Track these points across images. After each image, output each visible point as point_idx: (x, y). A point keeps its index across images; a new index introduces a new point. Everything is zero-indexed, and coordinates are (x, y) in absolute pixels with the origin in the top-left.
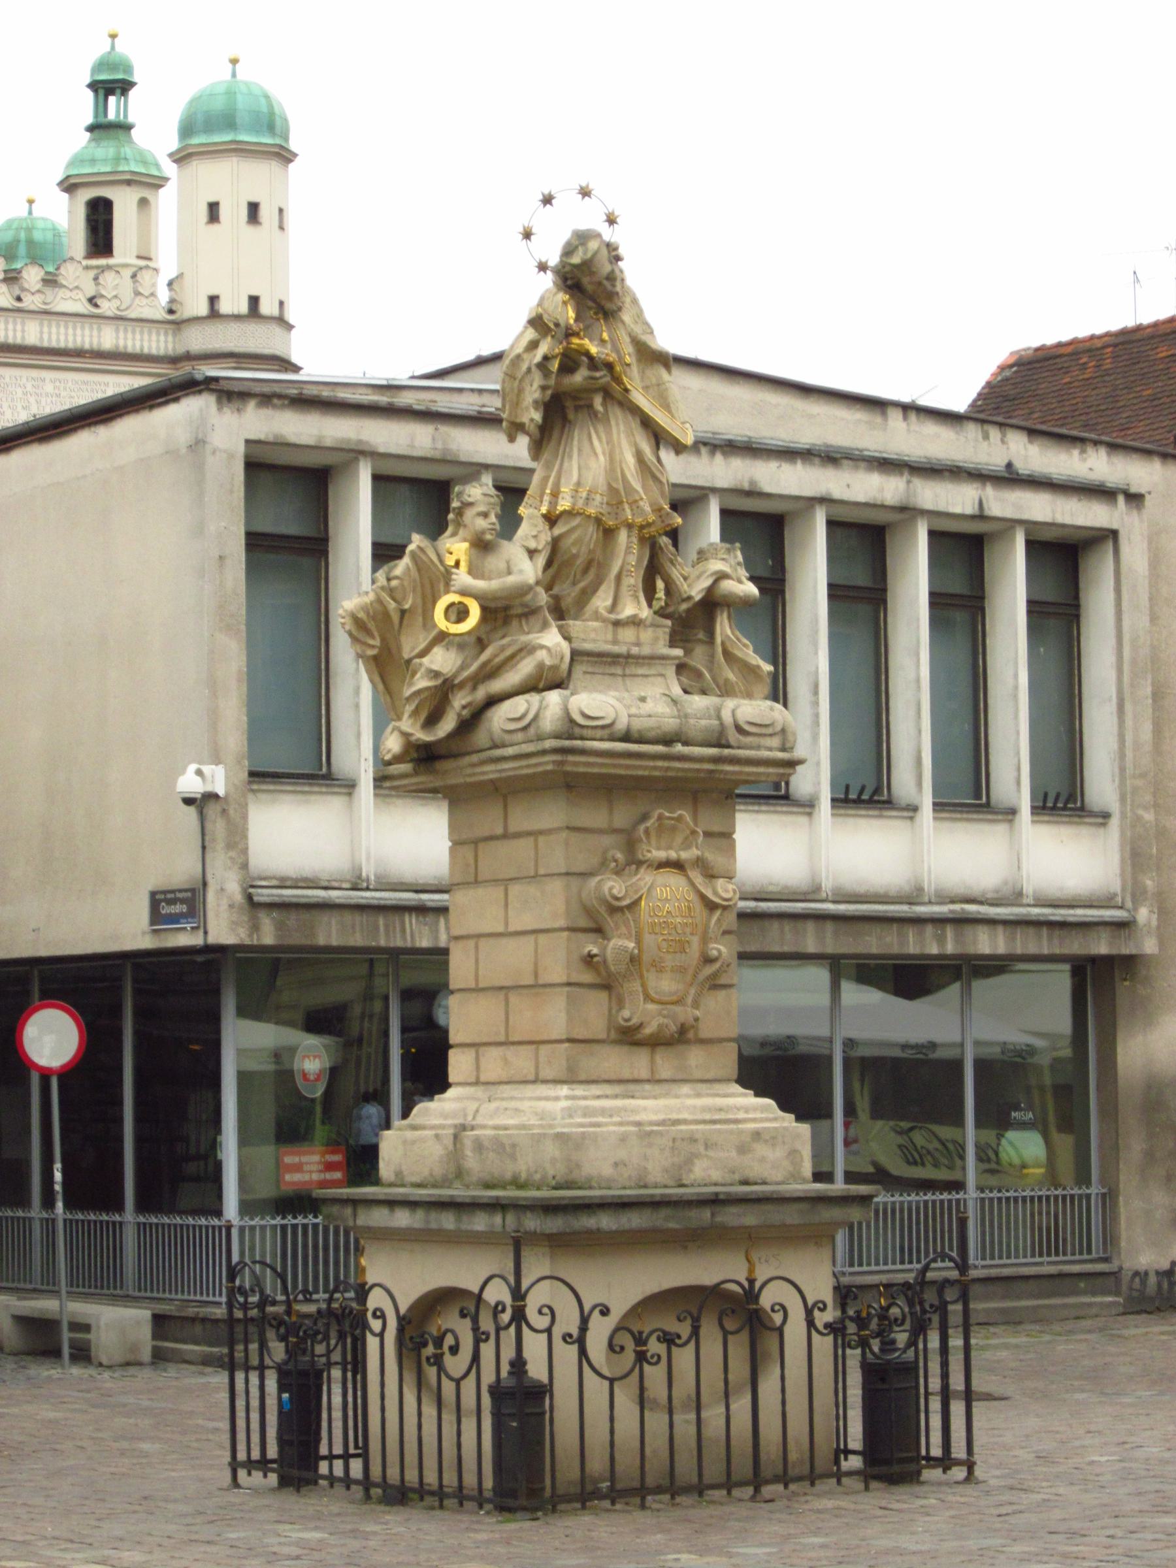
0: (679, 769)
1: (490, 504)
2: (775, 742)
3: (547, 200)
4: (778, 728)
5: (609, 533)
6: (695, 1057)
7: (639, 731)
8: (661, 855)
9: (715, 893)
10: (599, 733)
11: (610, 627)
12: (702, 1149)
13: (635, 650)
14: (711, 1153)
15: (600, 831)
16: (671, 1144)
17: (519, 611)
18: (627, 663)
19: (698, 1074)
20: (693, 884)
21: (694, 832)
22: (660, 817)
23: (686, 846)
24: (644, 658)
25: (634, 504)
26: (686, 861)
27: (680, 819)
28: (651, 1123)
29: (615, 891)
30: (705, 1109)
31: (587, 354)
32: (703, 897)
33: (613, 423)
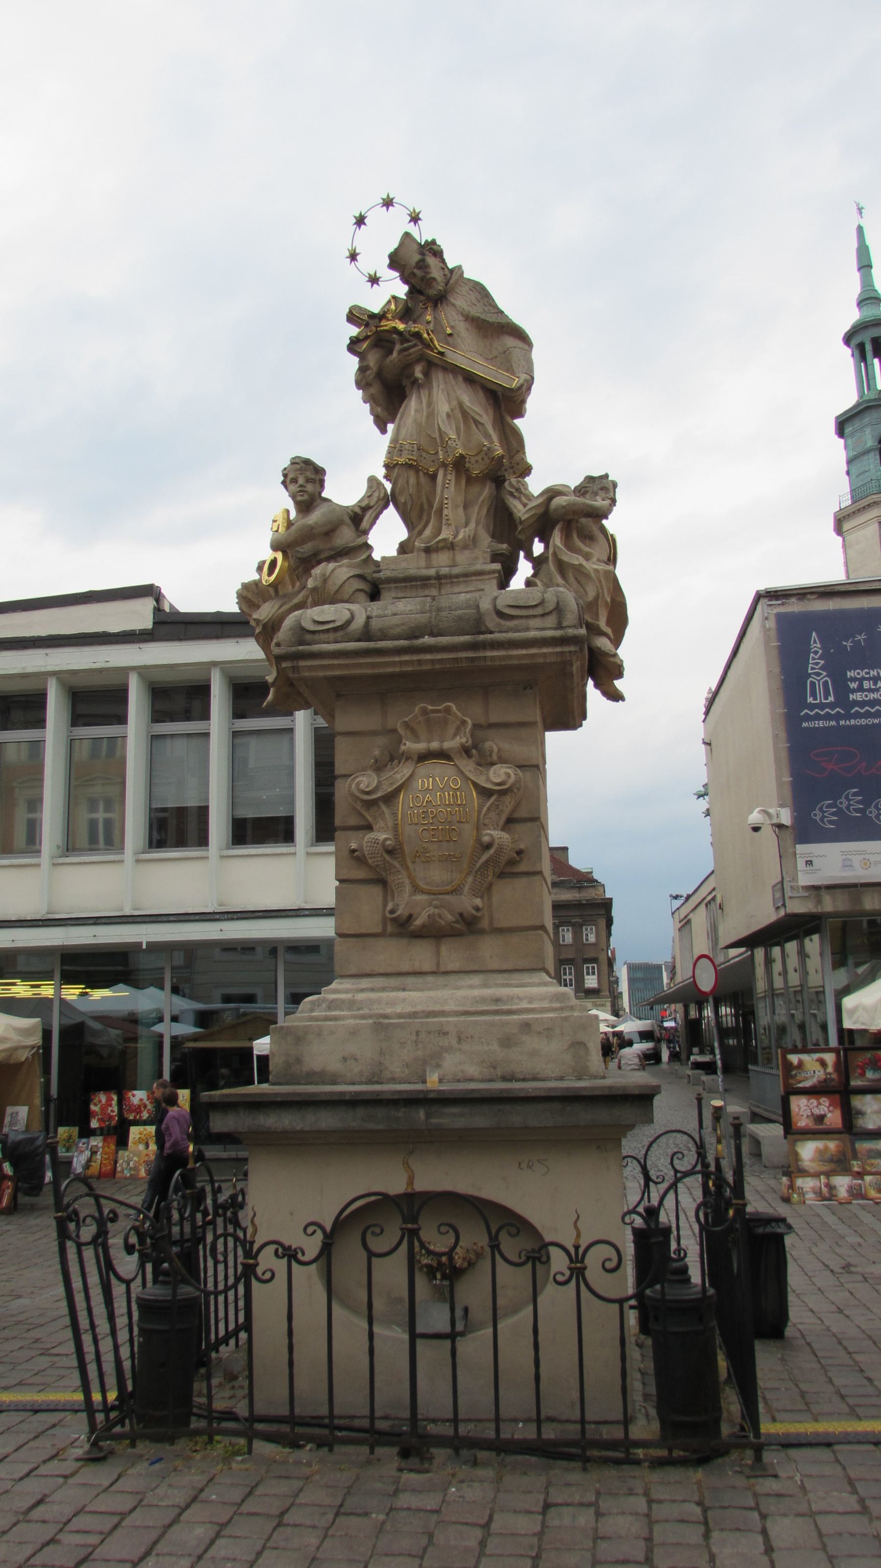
0: (432, 661)
1: (297, 470)
2: (551, 621)
3: (360, 221)
4: (550, 606)
5: (433, 477)
6: (489, 949)
7: (381, 630)
8: (421, 746)
9: (488, 780)
10: (332, 636)
11: (423, 554)
12: (454, 1043)
13: (444, 571)
14: (465, 1047)
15: (374, 733)
16: (414, 1038)
17: (326, 554)
18: (441, 584)
19: (495, 966)
20: (461, 773)
21: (464, 722)
22: (424, 712)
23: (455, 735)
24: (457, 576)
25: (445, 447)
26: (451, 749)
27: (448, 710)
28: (400, 1016)
29: (362, 786)
30: (483, 1000)
31: (395, 330)
32: (475, 785)
33: (435, 384)
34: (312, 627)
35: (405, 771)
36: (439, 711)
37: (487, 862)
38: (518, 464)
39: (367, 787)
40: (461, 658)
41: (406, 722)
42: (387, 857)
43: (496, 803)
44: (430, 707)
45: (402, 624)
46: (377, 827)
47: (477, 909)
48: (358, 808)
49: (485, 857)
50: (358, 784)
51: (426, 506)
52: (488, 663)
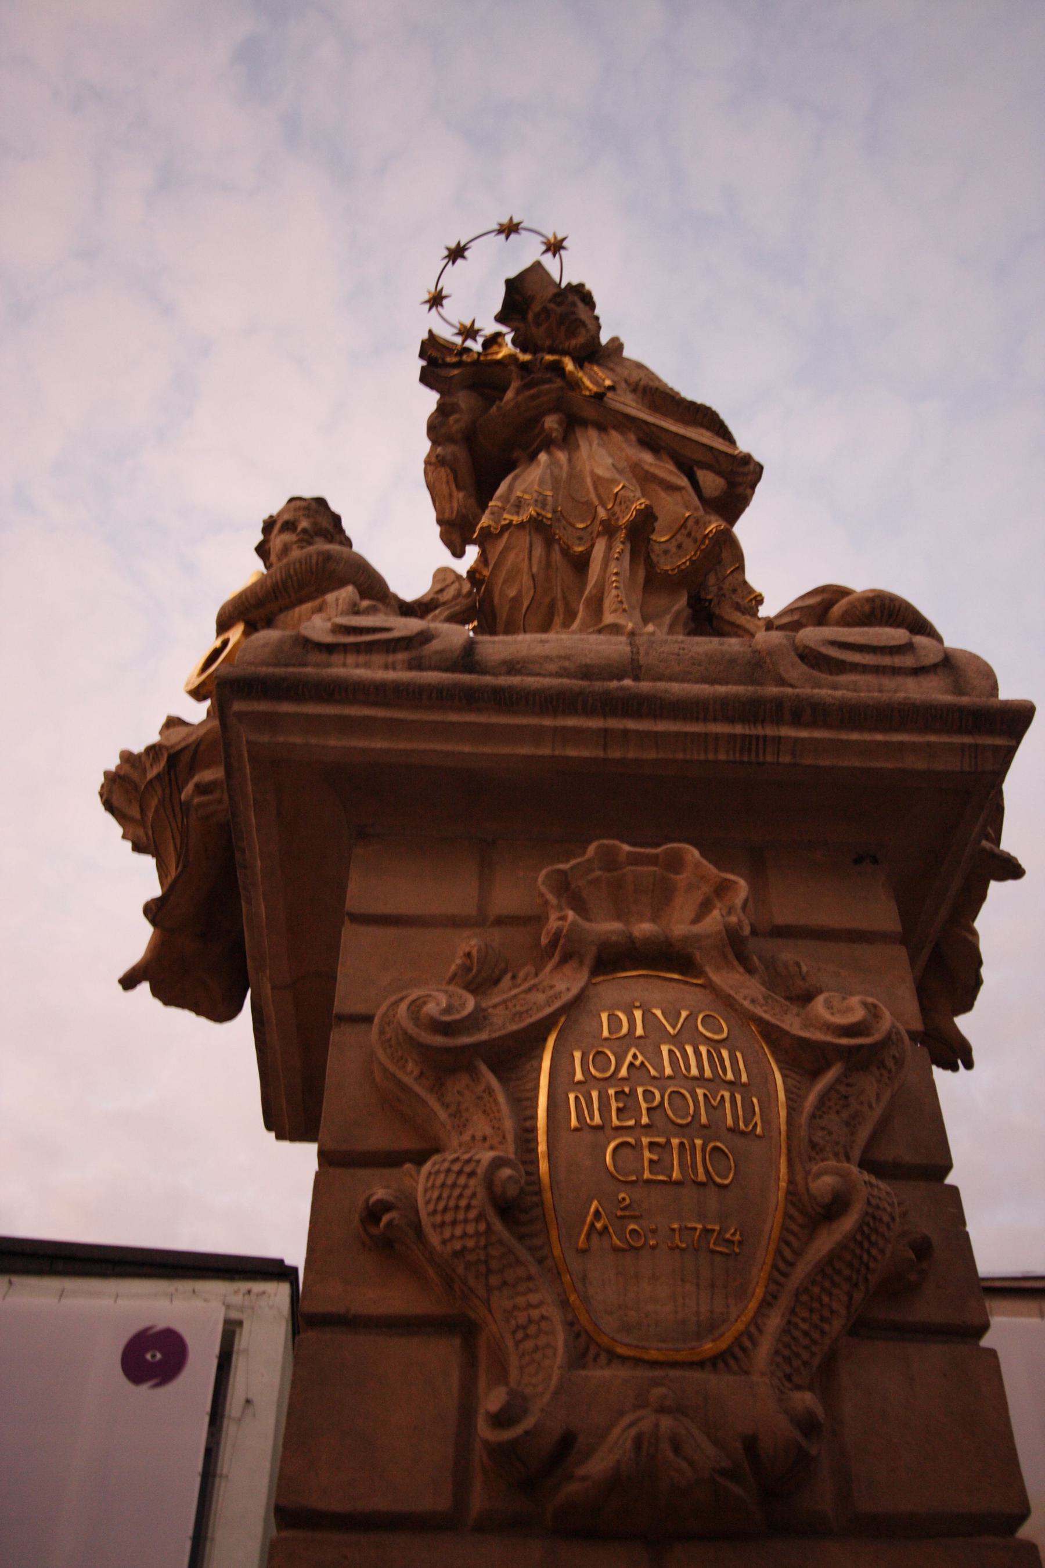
15: (456, 922)
22: (609, 861)
27: (675, 863)
29: (431, 1008)
32: (772, 1035)
34: (329, 639)
35: (561, 986)
36: (652, 860)
37: (832, 1258)
38: (734, 591)
39: (448, 1010)
40: (717, 737)
41: (562, 872)
42: (498, 1226)
43: (842, 1089)
44: (626, 848)
45: (567, 658)
46: (466, 1137)
47: (809, 1426)
48: (408, 1080)
49: (825, 1242)
50: (416, 1006)
51: (560, 605)
52: (786, 759)
